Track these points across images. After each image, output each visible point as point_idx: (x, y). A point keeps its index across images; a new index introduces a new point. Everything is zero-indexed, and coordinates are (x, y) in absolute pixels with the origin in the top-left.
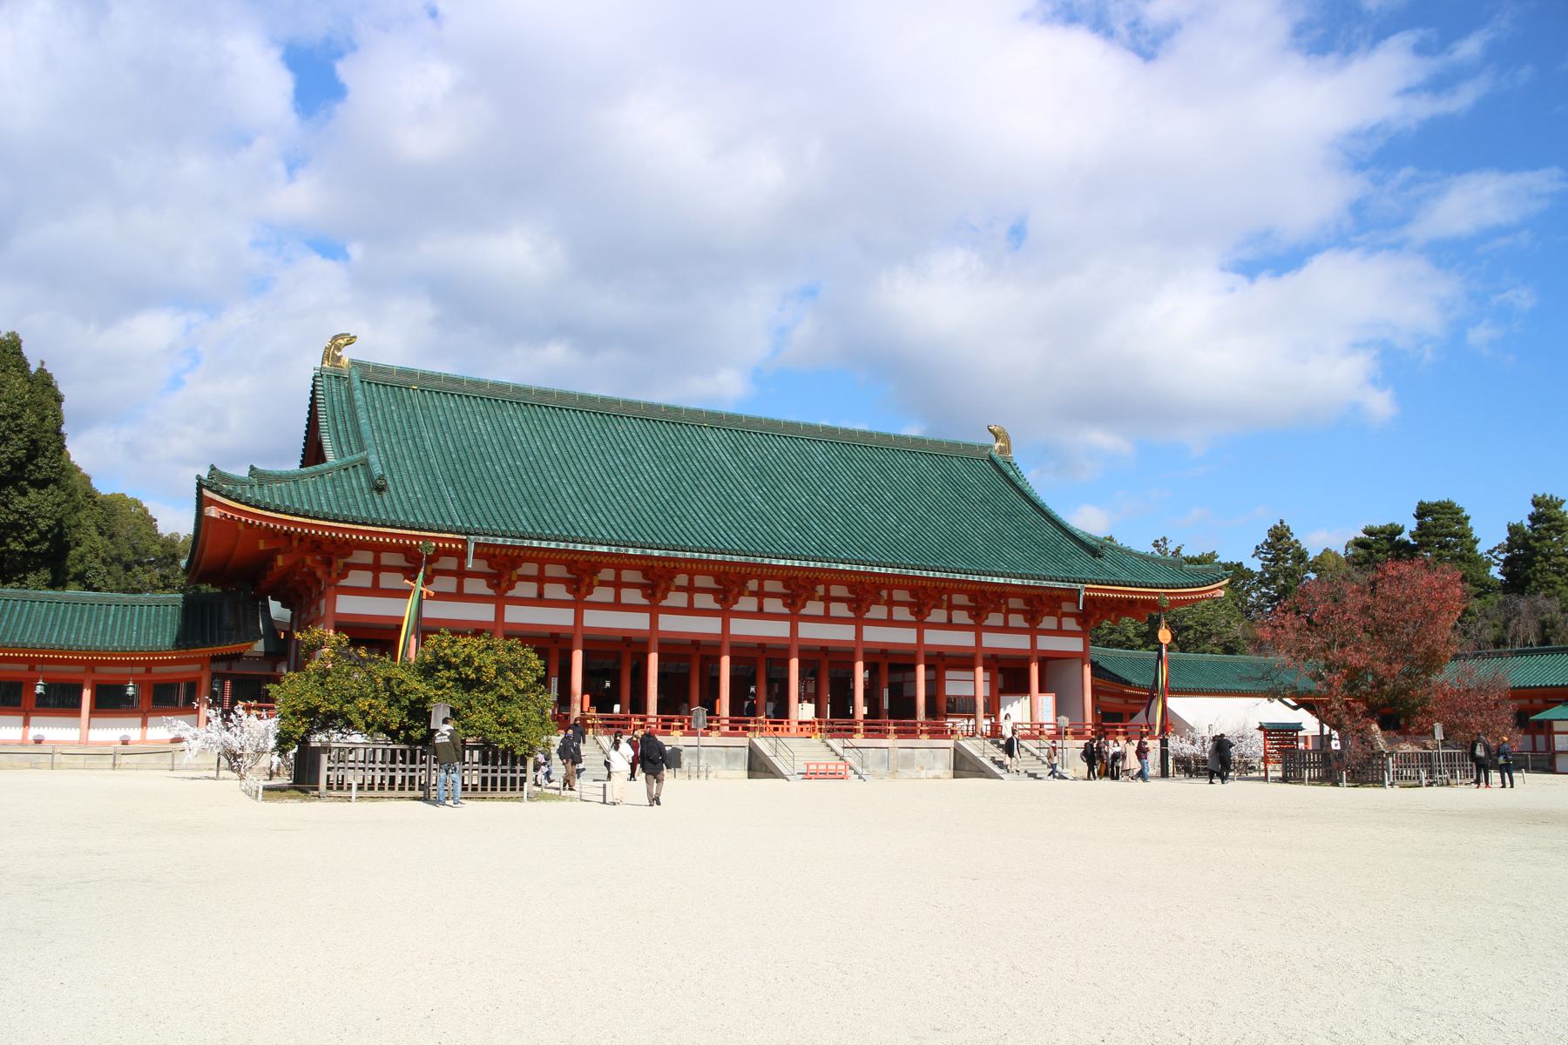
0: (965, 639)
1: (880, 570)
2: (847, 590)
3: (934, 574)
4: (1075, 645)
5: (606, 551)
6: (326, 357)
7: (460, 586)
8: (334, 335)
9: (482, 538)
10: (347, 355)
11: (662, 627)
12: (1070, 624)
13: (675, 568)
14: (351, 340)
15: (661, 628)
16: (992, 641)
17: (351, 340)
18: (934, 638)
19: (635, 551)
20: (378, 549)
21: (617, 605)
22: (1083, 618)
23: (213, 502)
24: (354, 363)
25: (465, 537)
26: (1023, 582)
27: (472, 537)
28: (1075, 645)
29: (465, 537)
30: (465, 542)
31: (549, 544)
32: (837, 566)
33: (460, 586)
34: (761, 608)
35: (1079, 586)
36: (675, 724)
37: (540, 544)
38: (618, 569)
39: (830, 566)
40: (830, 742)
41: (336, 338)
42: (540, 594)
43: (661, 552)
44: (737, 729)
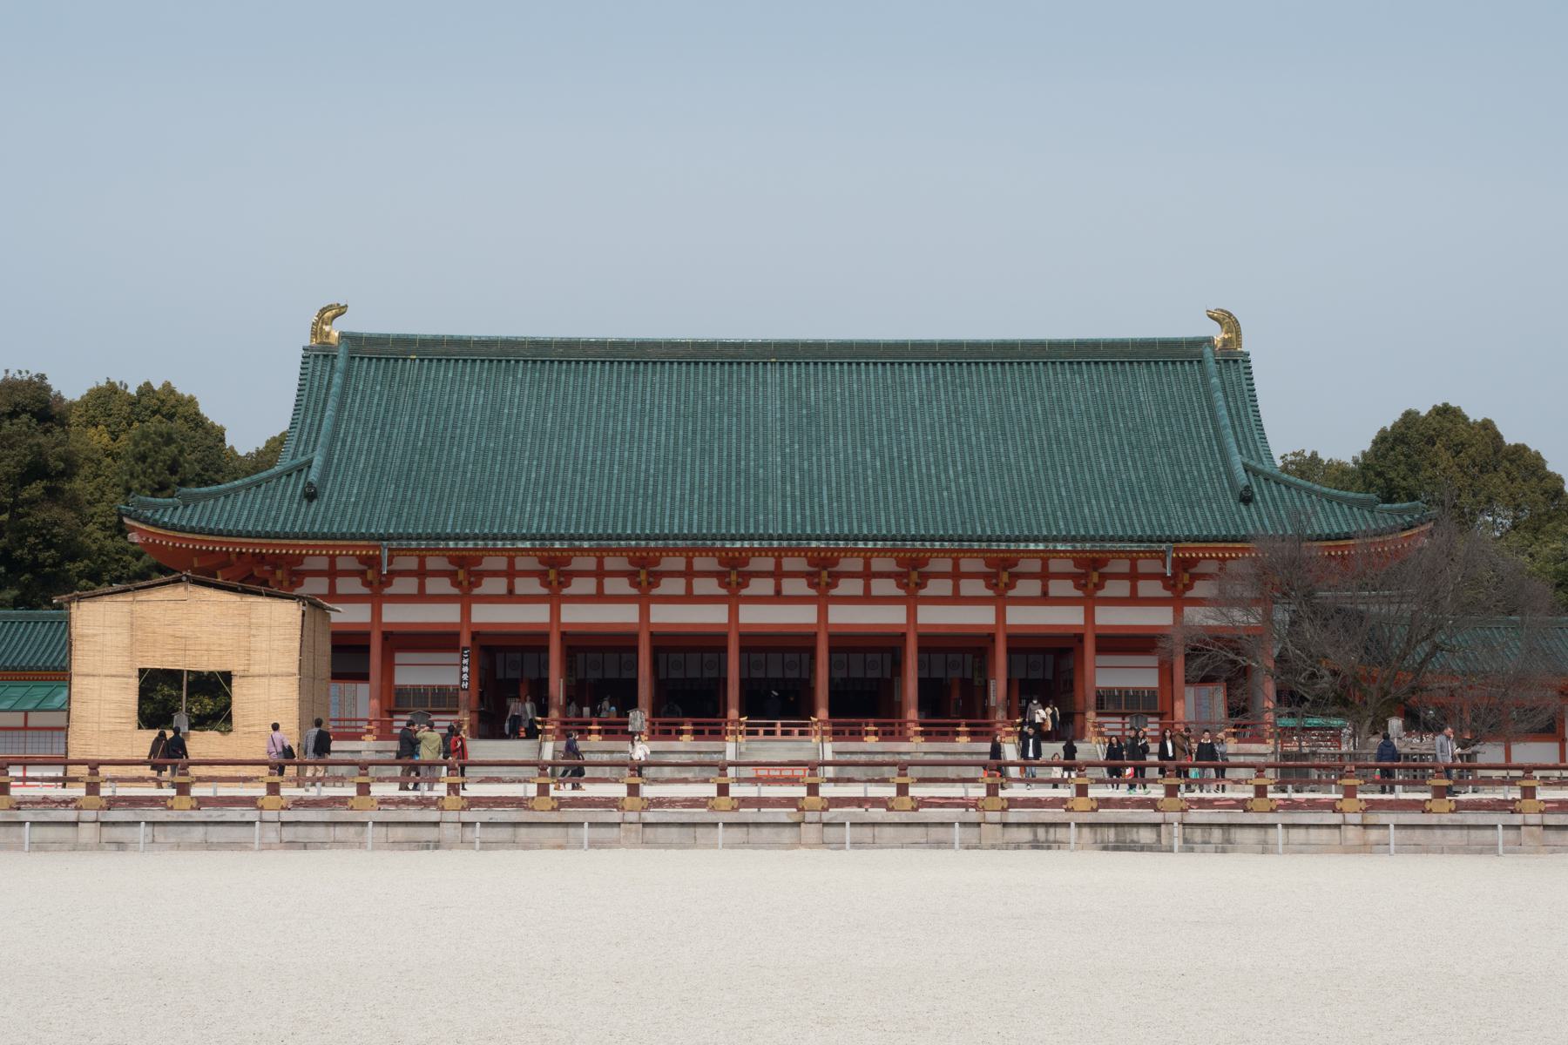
1: (866, 544)
2: (894, 562)
3: (941, 545)
5: (529, 546)
6: (314, 334)
7: (422, 586)
8: (321, 307)
9: (395, 543)
11: (653, 620)
14: (341, 310)
15: (653, 620)
16: (1109, 617)
17: (341, 310)
19: (561, 544)
21: (600, 597)
23: (133, 529)
24: (343, 336)
26: (1074, 547)
27: (385, 543)
31: (466, 544)
32: (809, 544)
33: (422, 586)
34: (778, 591)
35: (1164, 546)
36: (592, 727)
37: (457, 544)
39: (799, 544)
41: (324, 311)
42: (511, 591)
43: (592, 543)
44: (756, 733)
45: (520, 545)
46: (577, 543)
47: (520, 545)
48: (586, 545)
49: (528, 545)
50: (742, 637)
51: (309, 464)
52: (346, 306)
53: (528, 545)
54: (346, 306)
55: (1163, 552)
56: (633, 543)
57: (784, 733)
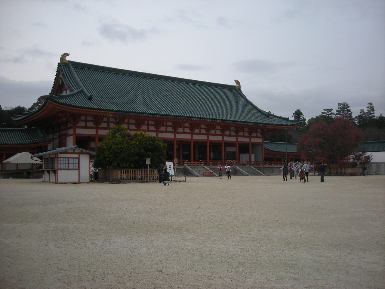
0: (233, 139)
4: (260, 140)
10: (68, 58)
12: (259, 135)
13: (145, 119)
14: (67, 54)
16: (241, 140)
17: (67, 54)
18: (227, 139)
20: (86, 115)
22: (263, 133)
24: (69, 61)
25: (116, 113)
27: (118, 113)
28: (260, 140)
29: (116, 113)
30: (115, 114)
38: (148, 121)
40: (205, 167)
45: (149, 116)
46: (162, 116)
47: (149, 116)
48: (164, 117)
49: (151, 116)
50: (177, 142)
51: (82, 91)
52: (69, 54)
53: (151, 116)
54: (69, 54)
55: (265, 127)
56: (174, 117)
57: (194, 164)
